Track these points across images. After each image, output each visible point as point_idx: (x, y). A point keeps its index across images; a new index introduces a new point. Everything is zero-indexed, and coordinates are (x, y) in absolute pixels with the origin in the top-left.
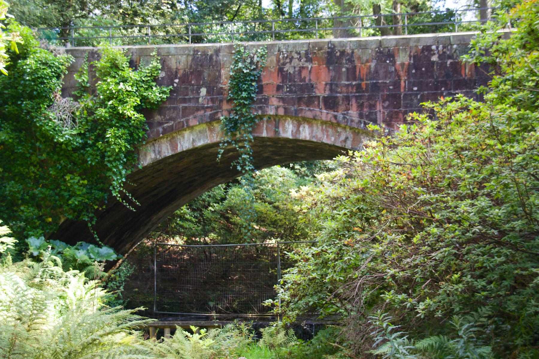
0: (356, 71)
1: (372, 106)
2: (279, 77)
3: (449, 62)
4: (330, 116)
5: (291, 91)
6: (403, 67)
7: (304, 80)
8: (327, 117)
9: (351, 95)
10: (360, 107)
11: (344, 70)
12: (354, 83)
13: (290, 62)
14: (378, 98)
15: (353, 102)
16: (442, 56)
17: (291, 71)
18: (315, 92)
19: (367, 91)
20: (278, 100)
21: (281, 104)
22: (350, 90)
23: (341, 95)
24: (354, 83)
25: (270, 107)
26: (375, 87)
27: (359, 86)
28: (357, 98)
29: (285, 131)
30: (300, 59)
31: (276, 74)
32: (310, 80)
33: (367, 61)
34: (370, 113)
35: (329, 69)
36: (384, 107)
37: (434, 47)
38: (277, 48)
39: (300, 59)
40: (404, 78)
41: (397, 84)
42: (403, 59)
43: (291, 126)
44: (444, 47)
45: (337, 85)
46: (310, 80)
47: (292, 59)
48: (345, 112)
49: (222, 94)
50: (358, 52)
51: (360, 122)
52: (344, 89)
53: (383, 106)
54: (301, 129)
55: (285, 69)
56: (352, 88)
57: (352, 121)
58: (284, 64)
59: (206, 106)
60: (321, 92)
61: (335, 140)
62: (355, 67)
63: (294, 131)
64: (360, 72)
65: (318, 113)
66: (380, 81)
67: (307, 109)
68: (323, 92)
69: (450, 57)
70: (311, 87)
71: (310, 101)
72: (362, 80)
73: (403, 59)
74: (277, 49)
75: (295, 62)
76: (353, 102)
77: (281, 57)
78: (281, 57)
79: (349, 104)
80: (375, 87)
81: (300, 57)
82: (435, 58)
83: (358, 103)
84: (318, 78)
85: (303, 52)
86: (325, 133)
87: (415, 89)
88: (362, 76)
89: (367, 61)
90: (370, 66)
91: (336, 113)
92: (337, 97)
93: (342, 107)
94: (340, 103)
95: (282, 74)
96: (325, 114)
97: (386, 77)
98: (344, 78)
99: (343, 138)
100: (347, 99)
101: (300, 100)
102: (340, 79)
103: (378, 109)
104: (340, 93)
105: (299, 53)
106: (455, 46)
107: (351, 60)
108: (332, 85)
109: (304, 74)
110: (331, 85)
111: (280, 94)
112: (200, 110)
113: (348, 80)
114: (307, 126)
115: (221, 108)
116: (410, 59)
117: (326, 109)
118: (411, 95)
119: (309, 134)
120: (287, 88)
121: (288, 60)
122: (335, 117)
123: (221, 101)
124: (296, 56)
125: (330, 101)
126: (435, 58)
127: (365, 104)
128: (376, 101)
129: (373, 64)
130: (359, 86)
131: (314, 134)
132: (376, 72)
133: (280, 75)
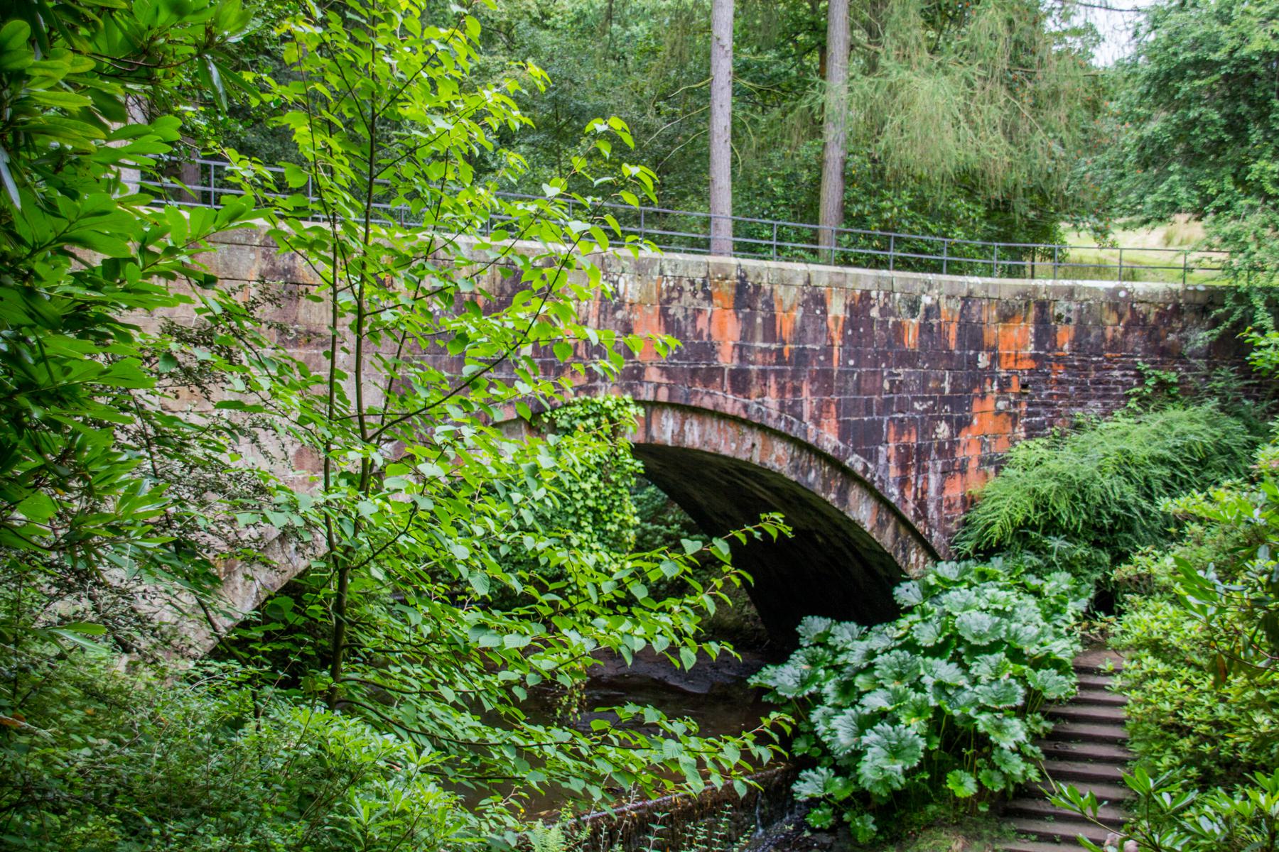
1: (797, 391)
3: (892, 320)
4: (738, 405)
7: (699, 335)
10: (781, 390)
11: (759, 320)
12: (774, 346)
13: (679, 299)
15: (772, 381)
16: (885, 311)
17: (680, 316)
19: (790, 363)
21: (664, 380)
24: (774, 346)
26: (801, 357)
27: (780, 351)
28: (779, 374)
29: (660, 429)
30: (694, 294)
31: (655, 320)
32: (710, 336)
33: (792, 308)
34: (795, 402)
36: (812, 394)
37: (874, 294)
39: (694, 294)
40: (838, 342)
41: (828, 351)
42: (837, 308)
43: (671, 422)
44: (887, 295)
45: (749, 348)
46: (710, 336)
47: (681, 291)
50: (780, 291)
51: (780, 418)
52: (759, 357)
54: (687, 427)
55: (671, 312)
57: (769, 415)
58: (669, 300)
60: (727, 360)
62: (774, 316)
65: (721, 400)
69: (892, 313)
70: (708, 350)
71: (711, 376)
72: (784, 343)
73: (837, 308)
74: (657, 269)
75: (687, 297)
76: (772, 381)
77: (664, 286)
80: (801, 357)
82: (874, 313)
84: (722, 333)
85: (699, 281)
87: (851, 362)
89: (792, 308)
92: (748, 371)
93: (755, 390)
97: (815, 340)
98: (759, 336)
99: (748, 445)
100: (763, 374)
101: (694, 372)
102: (753, 338)
104: (753, 363)
105: (692, 283)
106: (898, 296)
107: (769, 305)
108: (742, 350)
109: (702, 323)
110: (741, 348)
114: (695, 423)
117: (733, 393)
118: (846, 373)
121: (675, 294)
122: (746, 407)
124: (688, 287)
126: (874, 313)
127: (789, 385)
129: (798, 314)
130: (780, 351)
132: (803, 329)
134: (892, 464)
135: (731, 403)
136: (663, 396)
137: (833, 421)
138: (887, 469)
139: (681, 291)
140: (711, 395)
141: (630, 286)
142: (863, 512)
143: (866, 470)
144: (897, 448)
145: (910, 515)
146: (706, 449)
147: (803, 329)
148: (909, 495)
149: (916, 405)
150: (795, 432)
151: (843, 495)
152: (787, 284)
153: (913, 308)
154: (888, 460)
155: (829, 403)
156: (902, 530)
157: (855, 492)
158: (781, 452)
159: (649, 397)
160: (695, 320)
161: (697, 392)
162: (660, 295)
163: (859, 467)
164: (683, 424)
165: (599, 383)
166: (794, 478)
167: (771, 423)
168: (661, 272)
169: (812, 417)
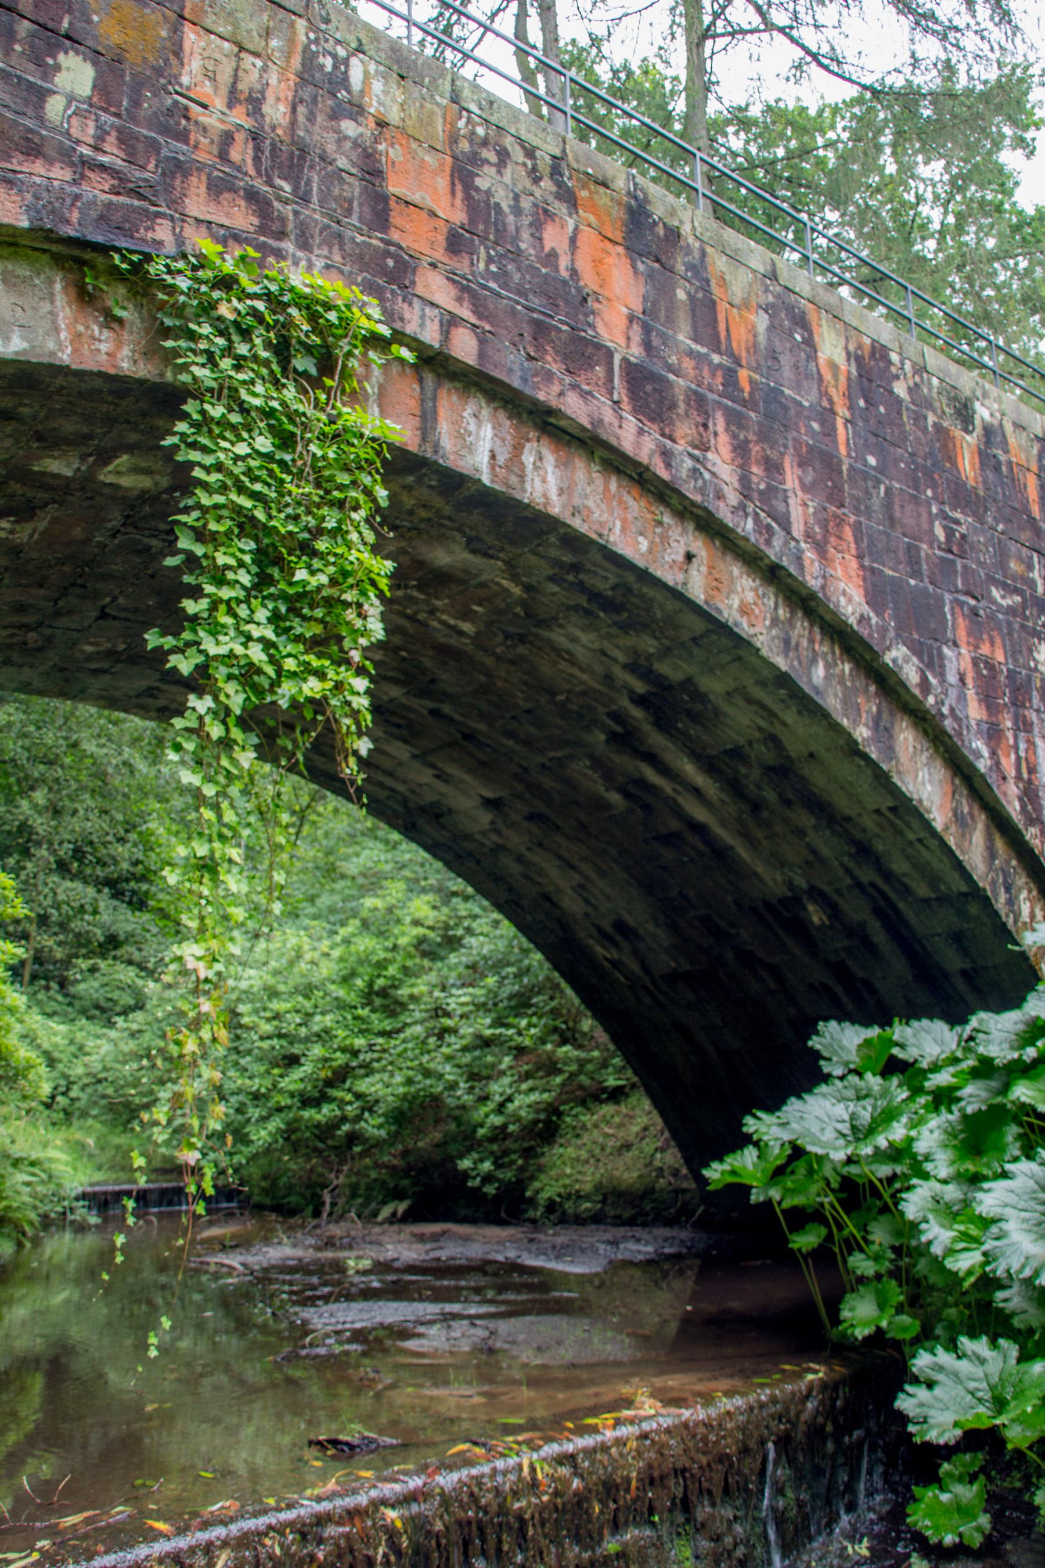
0: (715, 321)
1: (773, 467)
2: (458, 201)
5: (502, 277)
6: (836, 377)
8: (638, 445)
9: (711, 396)
10: (741, 449)
11: (681, 295)
14: (786, 447)
17: (502, 198)
18: (592, 326)
20: (453, 292)
21: (466, 313)
22: (706, 373)
23: (681, 381)
24: (716, 358)
25: (417, 304)
27: (730, 377)
35: (634, 267)
38: (448, 87)
43: (487, 431)
48: (696, 452)
49: (183, 136)
50: (719, 263)
51: (742, 507)
53: (800, 479)
54: (528, 458)
56: (713, 375)
57: (720, 496)
59: (86, 151)
61: (650, 551)
62: (714, 303)
63: (501, 459)
64: (728, 330)
65: (608, 416)
66: (787, 392)
67: (568, 380)
68: (622, 342)
78: (461, 123)
79: (705, 426)
81: (534, 169)
83: (734, 436)
86: (618, 512)
88: (734, 345)
90: (754, 327)
91: (668, 443)
93: (685, 430)
94: (682, 407)
95: (468, 197)
96: (633, 430)
103: (788, 486)
105: (530, 153)
109: (554, 238)
111: (463, 266)
112: (50, 161)
113: (696, 340)
114: (550, 458)
115: (175, 203)
116: (848, 360)
117: (636, 411)
119: (561, 492)
120: (490, 260)
123: (178, 168)
125: (649, 388)
128: (782, 454)
131: (577, 501)
133: (459, 194)
134: (971, 693)
135: (631, 435)
136: (464, 347)
137: (854, 564)
138: (962, 698)
139: (504, 156)
140: (585, 395)
141: (377, 86)
142: (926, 785)
143: (925, 685)
144: (975, 662)
145: (1013, 808)
146: (577, 523)
147: (773, 355)
148: (1008, 764)
149: (996, 593)
150: (775, 551)
151: (883, 732)
152: (735, 258)
153: (964, 413)
154: (962, 680)
155: (840, 521)
156: (1000, 844)
157: (906, 737)
158: (750, 597)
159: (431, 336)
160: (537, 226)
161: (549, 376)
162: (453, 139)
163: (911, 674)
164: (518, 449)
165: (289, 246)
166: (781, 663)
167: (724, 513)
168: (455, 100)
169: (808, 536)
